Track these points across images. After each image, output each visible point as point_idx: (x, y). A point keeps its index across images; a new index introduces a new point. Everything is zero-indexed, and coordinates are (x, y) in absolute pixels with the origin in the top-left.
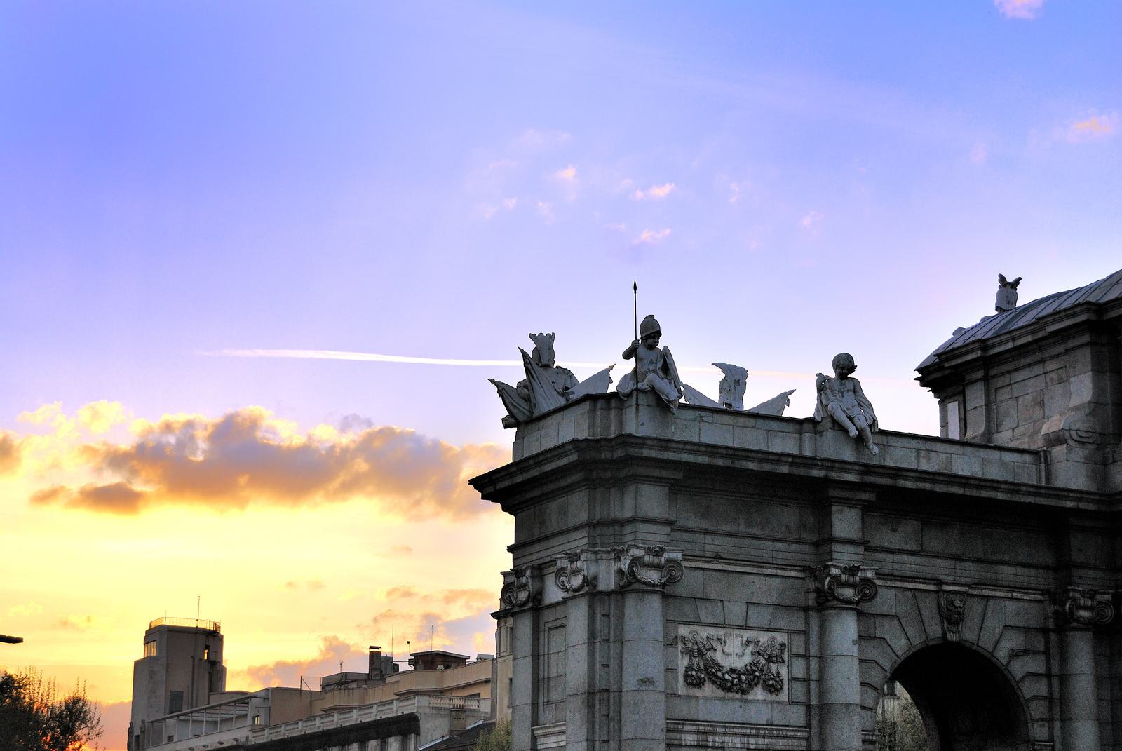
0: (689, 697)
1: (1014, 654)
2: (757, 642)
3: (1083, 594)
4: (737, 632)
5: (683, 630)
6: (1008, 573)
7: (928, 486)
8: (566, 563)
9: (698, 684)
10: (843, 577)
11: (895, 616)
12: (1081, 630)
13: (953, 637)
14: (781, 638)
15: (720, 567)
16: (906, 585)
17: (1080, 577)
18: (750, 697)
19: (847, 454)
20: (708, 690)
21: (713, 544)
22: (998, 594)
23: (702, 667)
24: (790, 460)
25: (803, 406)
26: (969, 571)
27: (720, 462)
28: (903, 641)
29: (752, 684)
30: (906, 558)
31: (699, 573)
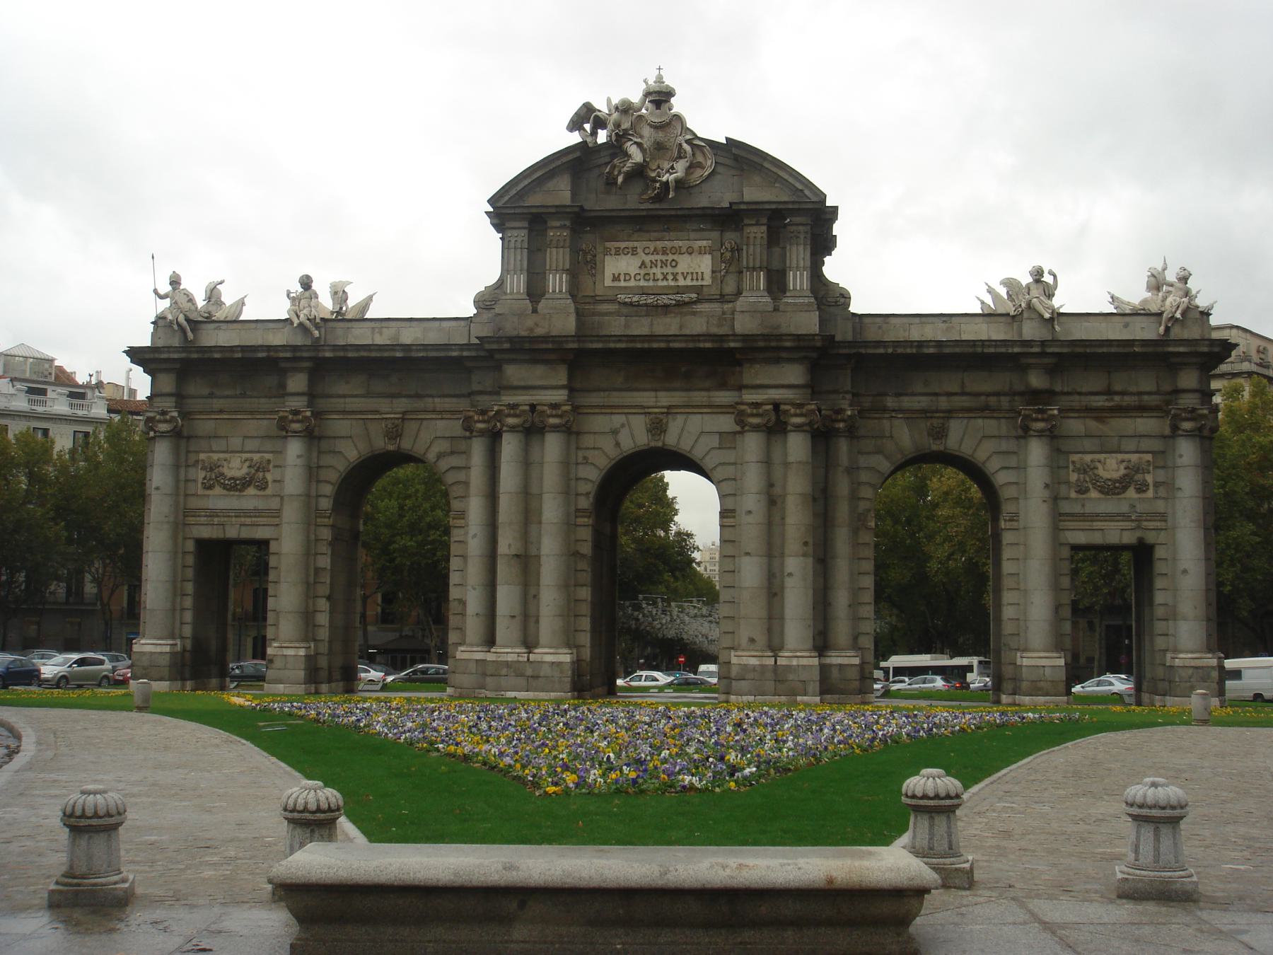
0: (204, 495)
1: (440, 456)
3: (476, 413)
5: (202, 456)
7: (342, 354)
9: (210, 487)
13: (391, 448)
18: (245, 493)
19: (299, 340)
20: (218, 490)
21: (217, 404)
23: (214, 477)
24: (239, 349)
25: (280, 310)
26: (402, 404)
27: (195, 356)
28: (355, 452)
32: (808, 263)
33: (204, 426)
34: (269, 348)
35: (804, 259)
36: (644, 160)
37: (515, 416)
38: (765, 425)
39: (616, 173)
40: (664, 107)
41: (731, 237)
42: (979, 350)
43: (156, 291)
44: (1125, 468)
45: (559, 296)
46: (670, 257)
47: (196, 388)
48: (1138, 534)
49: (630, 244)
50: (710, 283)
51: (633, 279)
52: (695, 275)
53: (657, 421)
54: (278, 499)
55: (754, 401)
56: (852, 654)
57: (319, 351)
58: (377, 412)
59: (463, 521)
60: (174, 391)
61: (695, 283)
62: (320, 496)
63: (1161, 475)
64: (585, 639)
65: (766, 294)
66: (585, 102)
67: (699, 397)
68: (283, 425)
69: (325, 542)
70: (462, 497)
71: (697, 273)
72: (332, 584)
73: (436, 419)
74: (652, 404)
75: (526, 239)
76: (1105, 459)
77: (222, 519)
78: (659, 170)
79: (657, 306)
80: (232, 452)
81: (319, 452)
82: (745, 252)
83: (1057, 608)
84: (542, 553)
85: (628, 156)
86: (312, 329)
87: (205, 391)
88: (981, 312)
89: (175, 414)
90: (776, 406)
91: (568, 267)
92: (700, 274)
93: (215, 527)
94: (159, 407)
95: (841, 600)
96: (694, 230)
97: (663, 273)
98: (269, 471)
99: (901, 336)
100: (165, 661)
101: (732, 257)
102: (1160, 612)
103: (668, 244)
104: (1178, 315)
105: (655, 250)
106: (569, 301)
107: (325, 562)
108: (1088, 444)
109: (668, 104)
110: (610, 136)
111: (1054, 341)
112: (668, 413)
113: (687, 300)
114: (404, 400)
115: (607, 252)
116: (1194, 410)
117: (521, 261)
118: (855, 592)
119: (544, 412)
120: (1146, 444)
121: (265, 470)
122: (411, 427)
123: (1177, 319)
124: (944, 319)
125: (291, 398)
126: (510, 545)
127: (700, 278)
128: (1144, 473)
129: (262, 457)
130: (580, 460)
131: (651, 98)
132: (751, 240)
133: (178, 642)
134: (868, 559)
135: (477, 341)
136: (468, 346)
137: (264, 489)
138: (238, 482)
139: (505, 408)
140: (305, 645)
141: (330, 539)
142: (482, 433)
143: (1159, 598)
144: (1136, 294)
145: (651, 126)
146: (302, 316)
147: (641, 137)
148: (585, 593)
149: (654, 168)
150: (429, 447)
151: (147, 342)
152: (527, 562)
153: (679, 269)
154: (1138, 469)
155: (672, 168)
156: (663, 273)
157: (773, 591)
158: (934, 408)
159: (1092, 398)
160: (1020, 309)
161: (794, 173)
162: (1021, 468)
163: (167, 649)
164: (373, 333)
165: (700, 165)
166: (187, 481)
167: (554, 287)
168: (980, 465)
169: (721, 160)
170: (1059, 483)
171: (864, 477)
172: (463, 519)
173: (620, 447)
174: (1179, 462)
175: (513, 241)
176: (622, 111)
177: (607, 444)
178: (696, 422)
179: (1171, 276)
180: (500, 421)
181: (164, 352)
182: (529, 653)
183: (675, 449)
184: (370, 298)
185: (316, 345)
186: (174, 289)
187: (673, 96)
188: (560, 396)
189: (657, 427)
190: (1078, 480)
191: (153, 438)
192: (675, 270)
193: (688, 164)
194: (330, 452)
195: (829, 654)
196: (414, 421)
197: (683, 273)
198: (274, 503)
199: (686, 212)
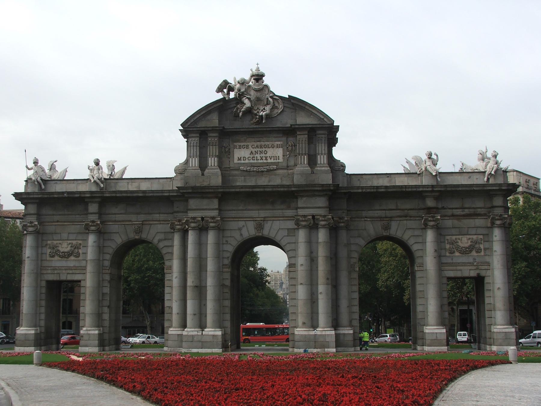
1: (160, 241)
5: (49, 242)
6: (157, 216)
7: (114, 195)
9: (53, 256)
10: (90, 224)
11: (118, 233)
12: (176, 232)
13: (137, 237)
14: (80, 242)
15: (60, 224)
16: (122, 223)
17: (177, 216)
18: (69, 259)
19: (94, 189)
20: (57, 258)
21: (56, 218)
22: (155, 223)
23: (55, 252)
25: (85, 175)
26: (142, 217)
27: (46, 196)
30: (119, 215)
31: (53, 226)
32: (326, 152)
33: (50, 228)
34: (80, 193)
35: (324, 150)
36: (251, 106)
37: (194, 222)
38: (308, 225)
39: (239, 112)
40: (260, 82)
41: (291, 140)
42: (404, 190)
43: (27, 167)
44: (471, 242)
45: (214, 168)
46: (264, 149)
47: (46, 211)
48: (478, 272)
49: (246, 144)
50: (282, 161)
51: (247, 159)
52: (275, 157)
53: (259, 224)
54: (85, 261)
55: (303, 214)
56: (349, 329)
57: (103, 193)
58: (130, 221)
59: (170, 270)
60: (36, 212)
61: (275, 161)
62: (105, 260)
63: (487, 245)
64: (228, 324)
65: (308, 166)
66: (224, 79)
67: (278, 213)
68: (87, 227)
69: (107, 281)
70: (170, 260)
71: (276, 156)
72: (110, 301)
73: (158, 224)
74: (258, 216)
75: (198, 142)
76: (462, 238)
77: (59, 271)
78: (258, 110)
79: (258, 172)
81: (104, 240)
82: (298, 147)
83: (441, 306)
84: (208, 285)
86: (100, 183)
87: (51, 212)
88: (404, 172)
89: (36, 223)
90: (313, 217)
91: (217, 154)
92: (277, 157)
94: (29, 220)
95: (344, 304)
96: (274, 137)
97: (261, 157)
98: (80, 249)
99: (369, 184)
100: (32, 338)
101: (292, 149)
102: (487, 307)
103: (263, 143)
104: (493, 173)
105: (257, 146)
106: (219, 170)
107: (107, 290)
108: (454, 231)
109: (261, 81)
110: (236, 95)
111: (438, 185)
112: (264, 220)
113: (272, 169)
114: (143, 215)
115: (235, 147)
116: (501, 215)
117: (196, 152)
118: (350, 300)
119: (207, 220)
120: (480, 231)
121: (79, 248)
122: (146, 228)
123: (492, 174)
124: (388, 175)
125: (90, 215)
126: (193, 282)
127: (277, 159)
128: (479, 244)
130: (224, 242)
131: (254, 78)
132: (301, 142)
133: (38, 328)
134: (356, 285)
135: (177, 189)
136: (173, 191)
137: (78, 257)
138: (66, 254)
139: (189, 219)
140: (98, 329)
141: (109, 280)
142: (179, 230)
143: (487, 301)
144: (474, 163)
145: (255, 90)
146: (95, 178)
147: (250, 95)
148: (227, 303)
149: (256, 109)
150: (154, 237)
151: (22, 190)
152: (200, 289)
153: (268, 155)
154: (477, 242)
155: (264, 109)
156: (261, 157)
157: (313, 300)
158: (384, 216)
159: (454, 210)
160: (422, 171)
161: (319, 111)
162: (424, 242)
163: (33, 332)
164: (128, 184)
165: (277, 108)
166: (42, 254)
167: (211, 163)
168: (405, 241)
169: (286, 105)
170: (441, 249)
171: (353, 248)
172: (171, 269)
173: (242, 236)
174: (495, 239)
175: (192, 143)
176: (241, 83)
177: (237, 235)
178: (277, 224)
179: (489, 155)
180: (187, 225)
181: (32, 195)
182: (202, 331)
183: (267, 237)
184: (125, 168)
185: (102, 191)
186: (35, 165)
187: (264, 76)
188: (215, 213)
189: (260, 227)
190: (450, 248)
191: (26, 234)
192: (266, 155)
193: (271, 107)
194: (109, 240)
195: (339, 329)
196: (147, 225)
197: (270, 157)
198: (83, 263)
199: (271, 129)
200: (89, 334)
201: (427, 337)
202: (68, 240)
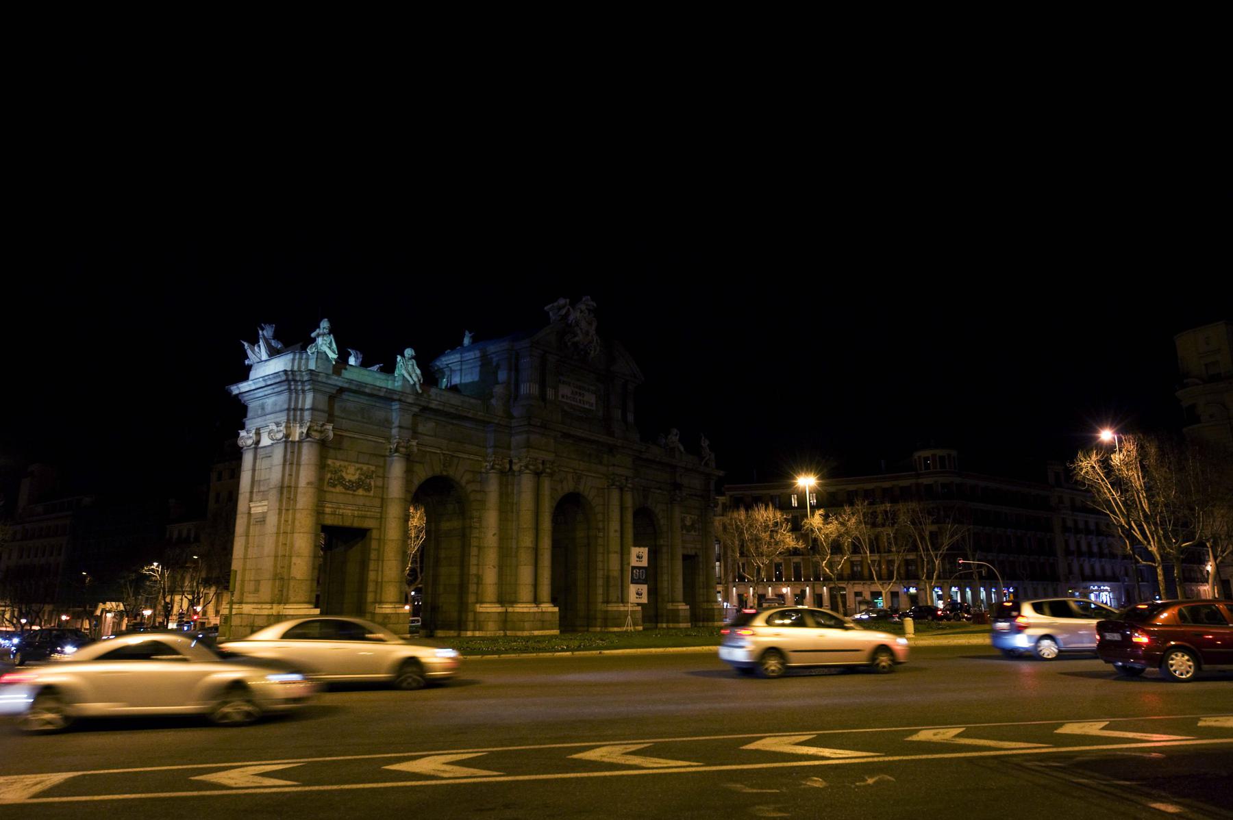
1: (468, 483)
2: (362, 469)
4: (353, 464)
8: (274, 427)
9: (334, 486)
13: (445, 473)
14: (373, 468)
18: (356, 493)
19: (408, 390)
20: (339, 489)
23: (336, 478)
24: (385, 390)
27: (353, 387)
29: (359, 487)
59: (478, 524)
80: (351, 462)
85: (575, 335)
90: (627, 477)
93: (337, 516)
110: (572, 321)
121: (371, 477)
129: (369, 468)
188: (550, 457)
200: (398, 614)
201: (681, 614)
202: (357, 462)
